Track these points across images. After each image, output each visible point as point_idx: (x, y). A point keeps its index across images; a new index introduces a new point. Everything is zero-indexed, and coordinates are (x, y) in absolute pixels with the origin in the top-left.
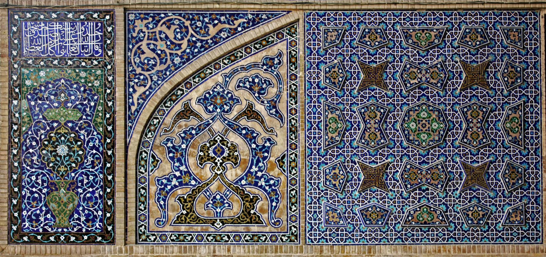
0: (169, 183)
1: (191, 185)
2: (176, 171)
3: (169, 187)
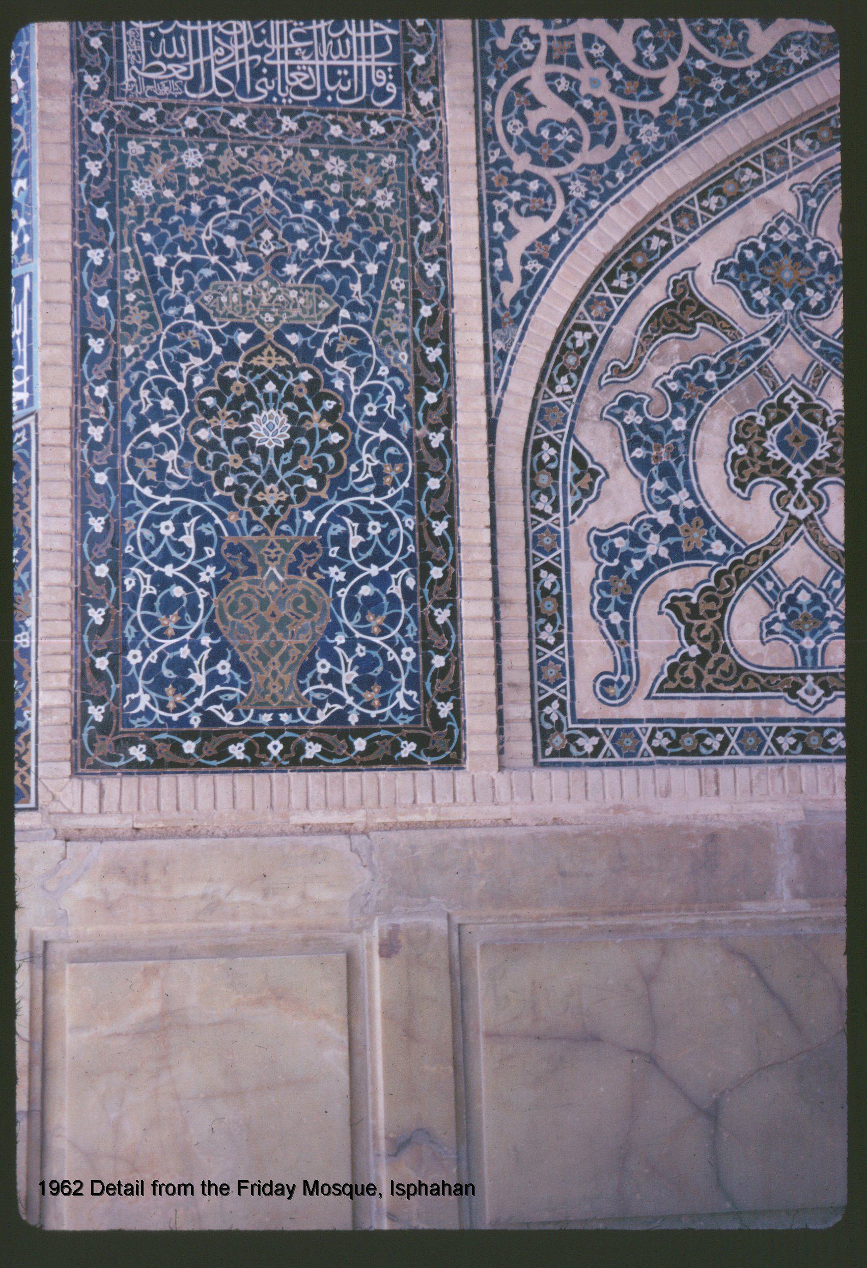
0: (636, 550)
1: (711, 556)
2: (658, 508)
3: (638, 565)
